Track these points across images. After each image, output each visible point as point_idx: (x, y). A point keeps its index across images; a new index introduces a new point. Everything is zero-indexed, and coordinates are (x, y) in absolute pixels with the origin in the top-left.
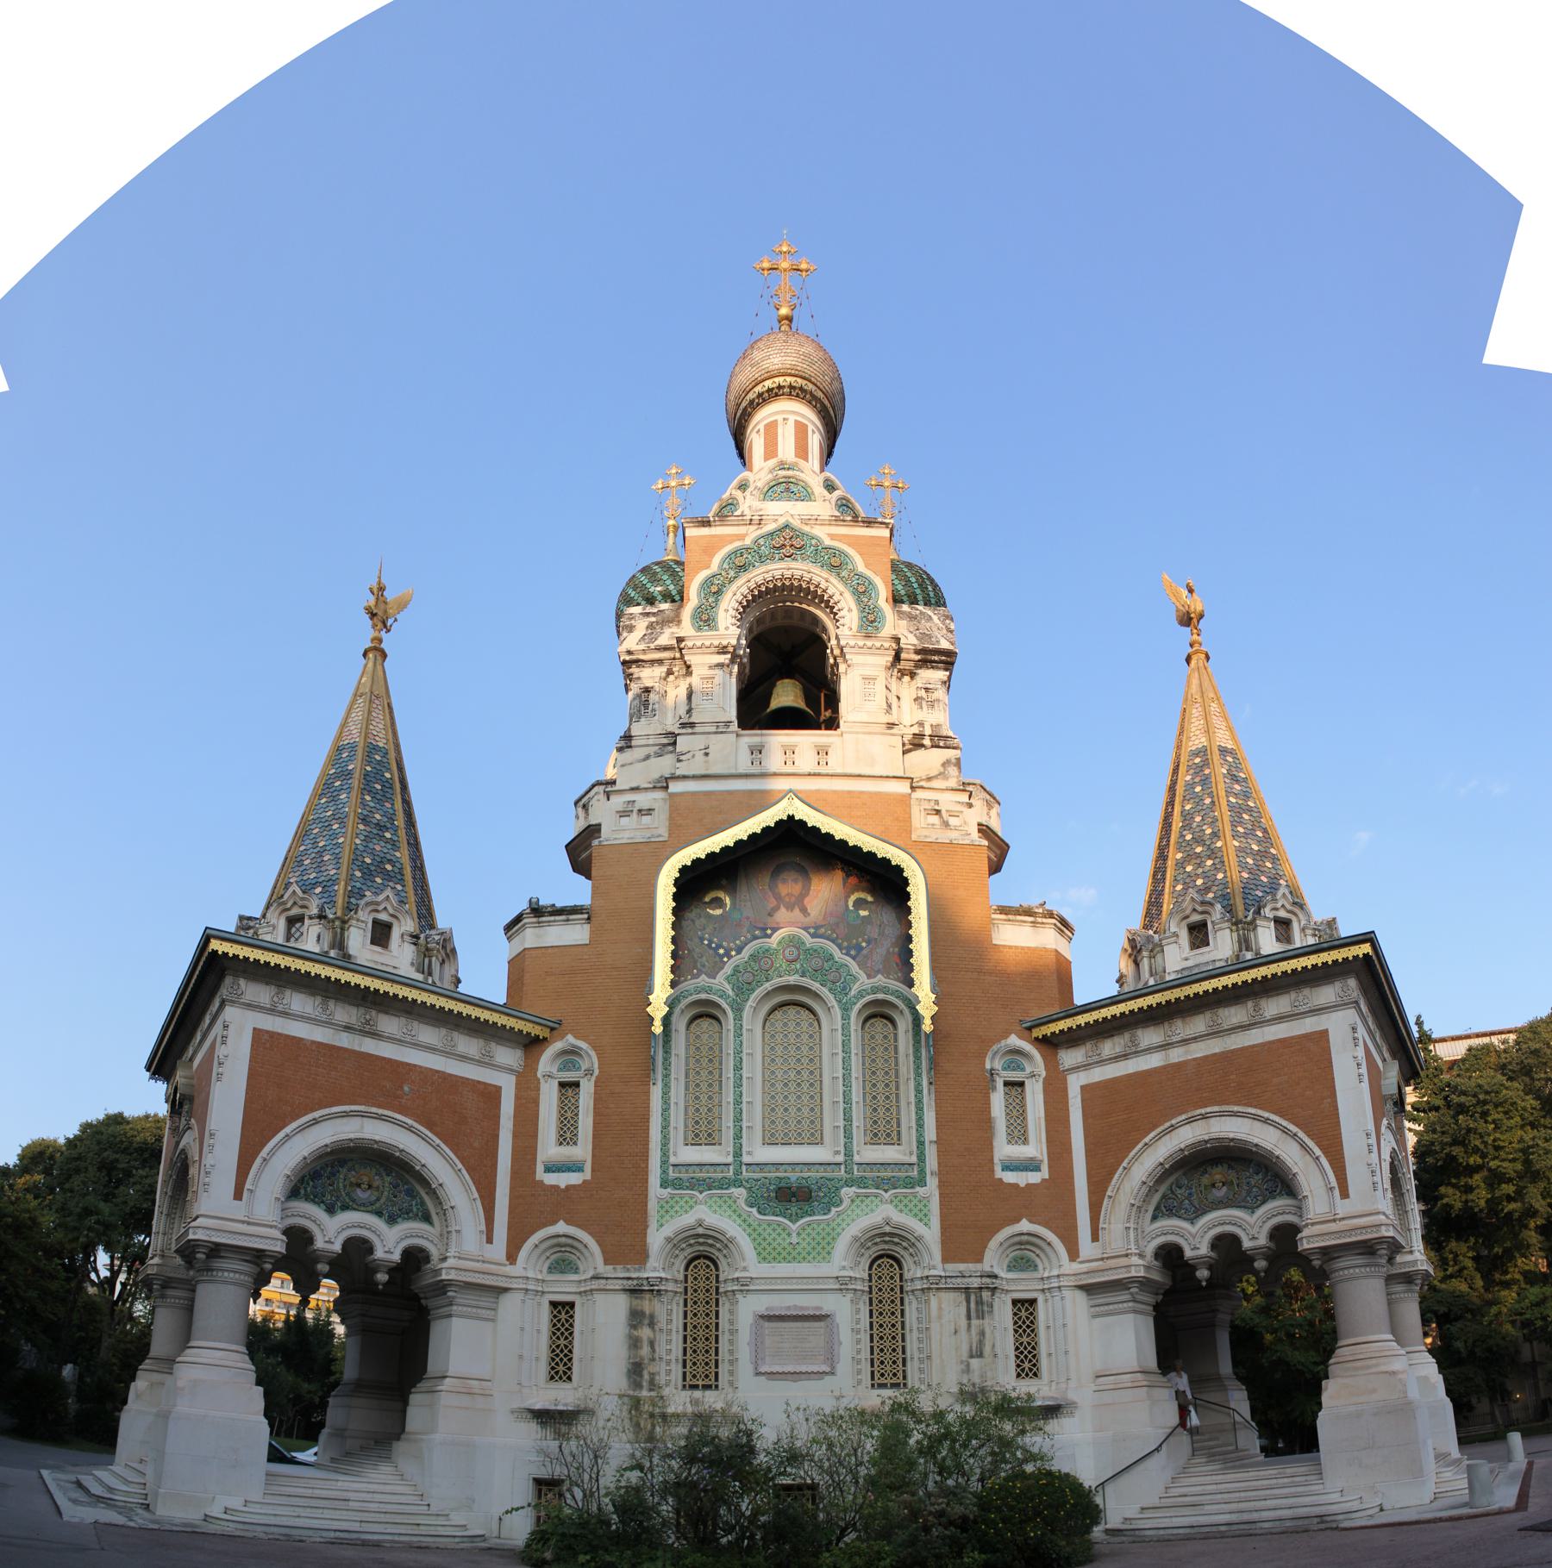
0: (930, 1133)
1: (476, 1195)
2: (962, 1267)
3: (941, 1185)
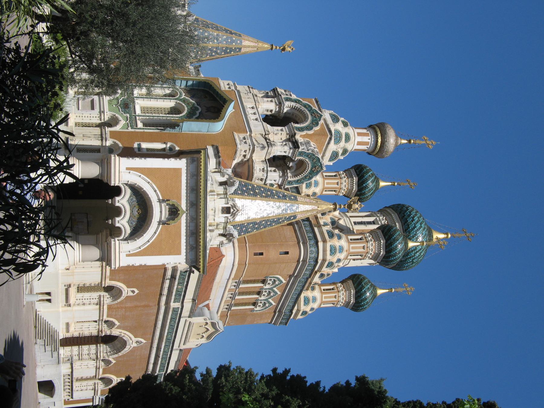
0: (146, 131)
3: (132, 132)
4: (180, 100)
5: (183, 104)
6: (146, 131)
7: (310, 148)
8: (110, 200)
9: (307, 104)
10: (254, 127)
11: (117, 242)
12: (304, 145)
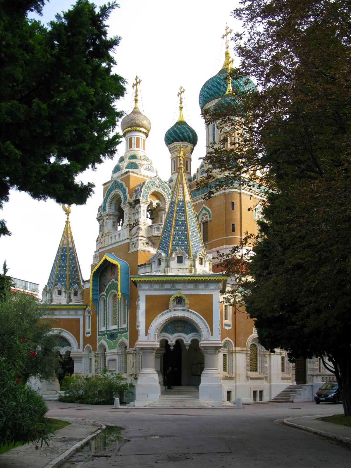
0: (129, 321)
1: (76, 340)
2: (131, 349)
4: (107, 295)
5: (110, 293)
6: (129, 321)
7: (139, 190)
8: (171, 348)
9: (107, 192)
10: (124, 236)
11: (202, 342)
12: (137, 195)
